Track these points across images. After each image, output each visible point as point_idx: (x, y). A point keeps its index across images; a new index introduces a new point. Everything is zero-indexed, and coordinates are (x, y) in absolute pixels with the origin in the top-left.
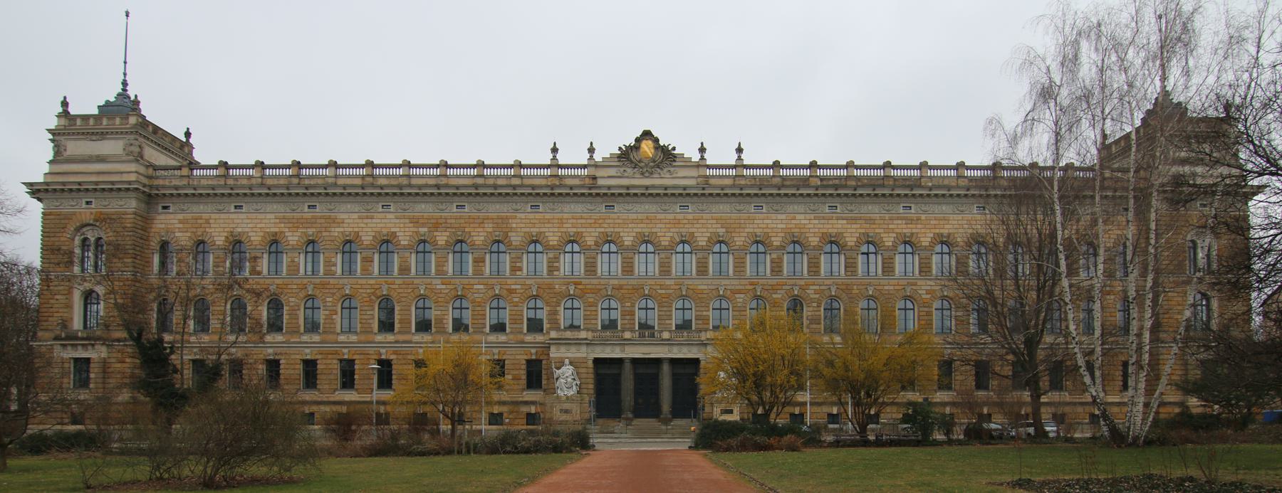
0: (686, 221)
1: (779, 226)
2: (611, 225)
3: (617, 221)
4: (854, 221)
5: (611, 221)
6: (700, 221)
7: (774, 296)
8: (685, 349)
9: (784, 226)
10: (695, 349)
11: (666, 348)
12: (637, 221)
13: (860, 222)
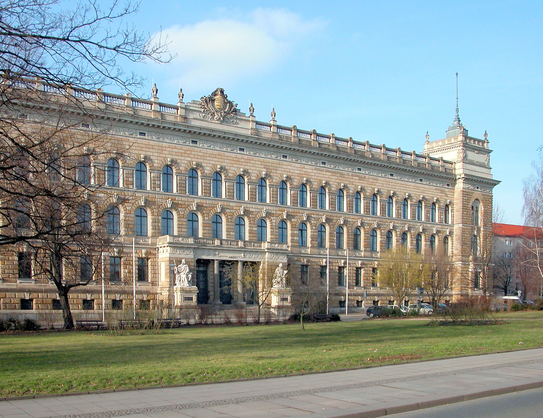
0: (243, 160)
1: (296, 172)
2: (196, 156)
3: (199, 154)
4: (334, 174)
5: (196, 153)
6: (252, 162)
9: (298, 172)
12: (213, 155)
13: (337, 175)
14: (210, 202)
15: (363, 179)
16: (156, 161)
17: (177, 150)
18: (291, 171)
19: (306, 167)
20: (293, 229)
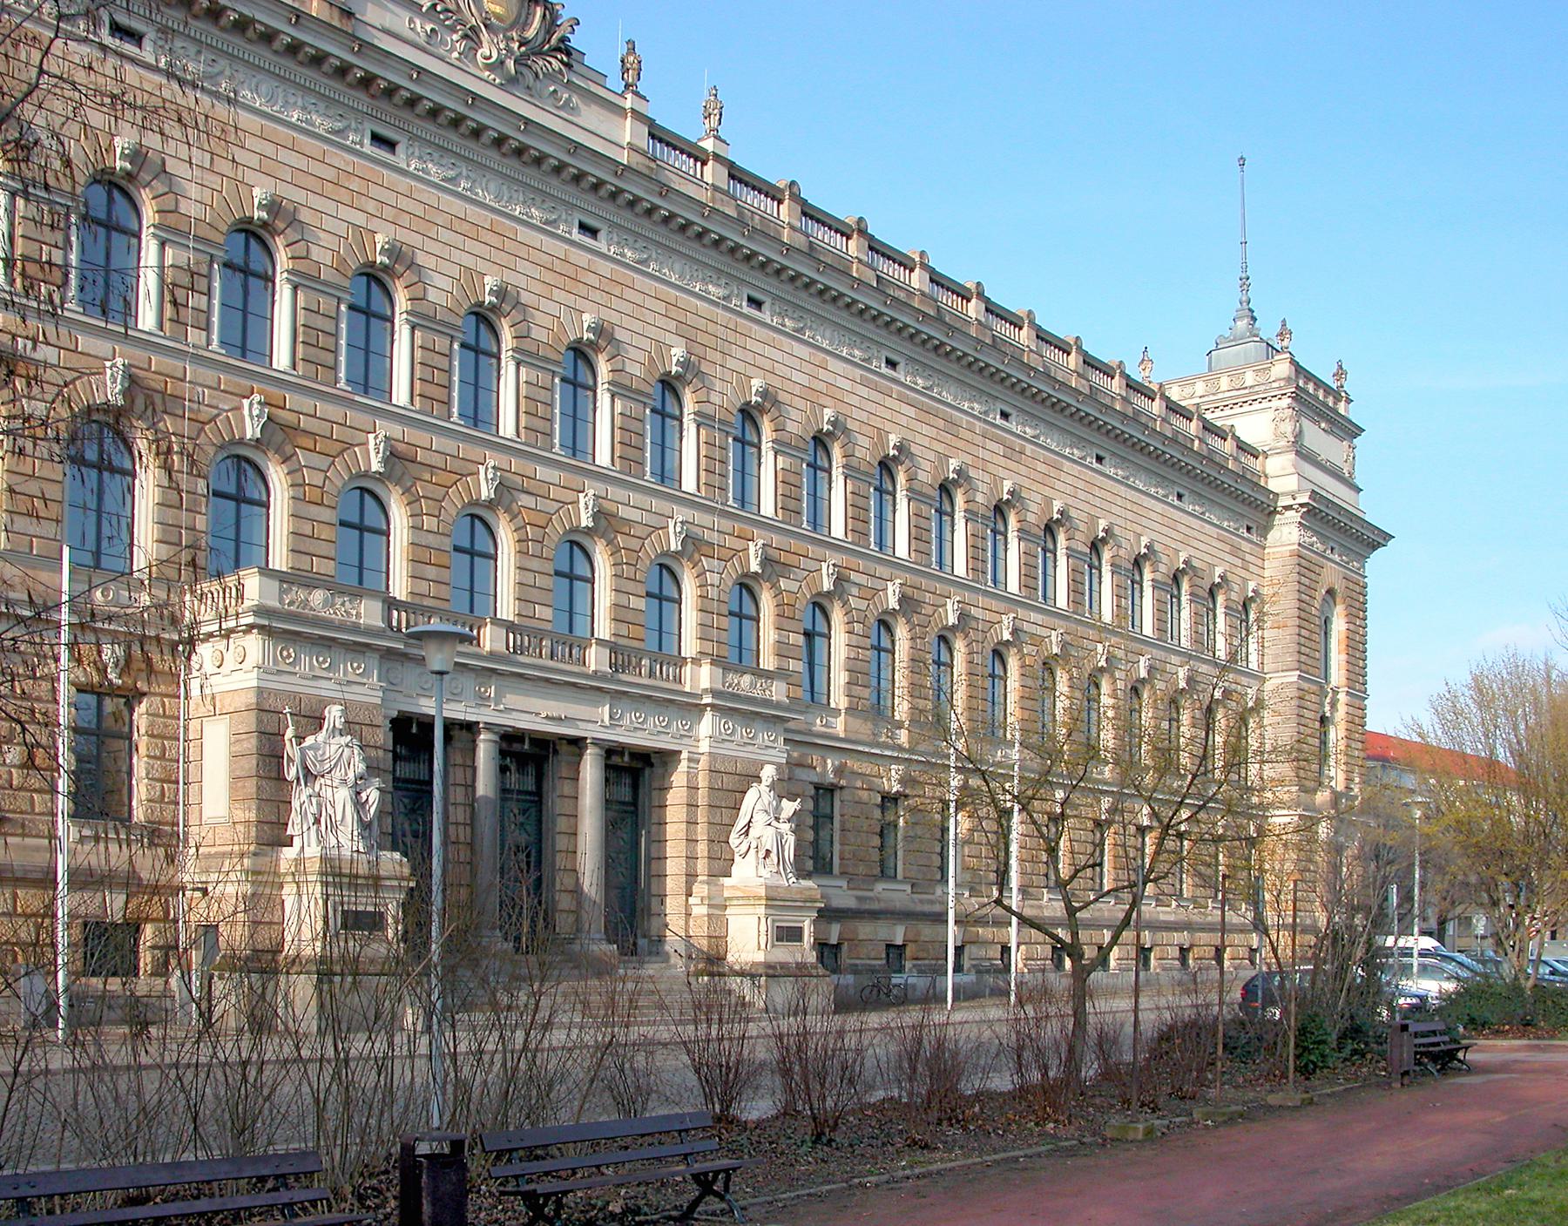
0: (592, 280)
2: (388, 213)
3: (404, 203)
6: (629, 294)
14: (449, 445)
15: (1016, 456)
16: (193, 191)
17: (301, 163)
18: (780, 369)
19: (834, 364)
20: (787, 624)
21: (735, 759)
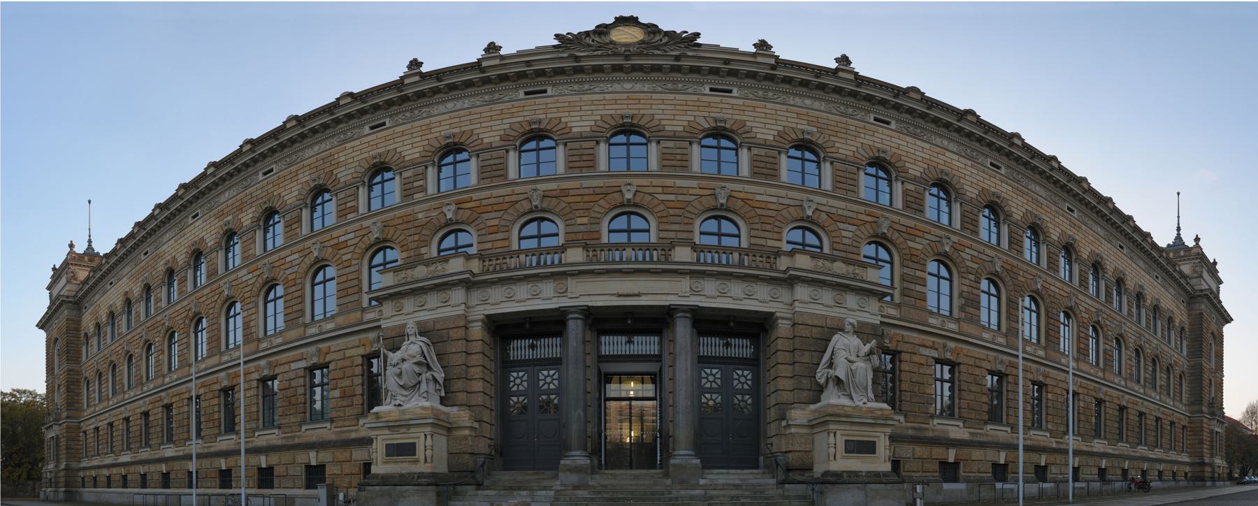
7: (911, 244)
8: (736, 289)
10: (762, 291)
11: (685, 284)
21: (826, 317)
